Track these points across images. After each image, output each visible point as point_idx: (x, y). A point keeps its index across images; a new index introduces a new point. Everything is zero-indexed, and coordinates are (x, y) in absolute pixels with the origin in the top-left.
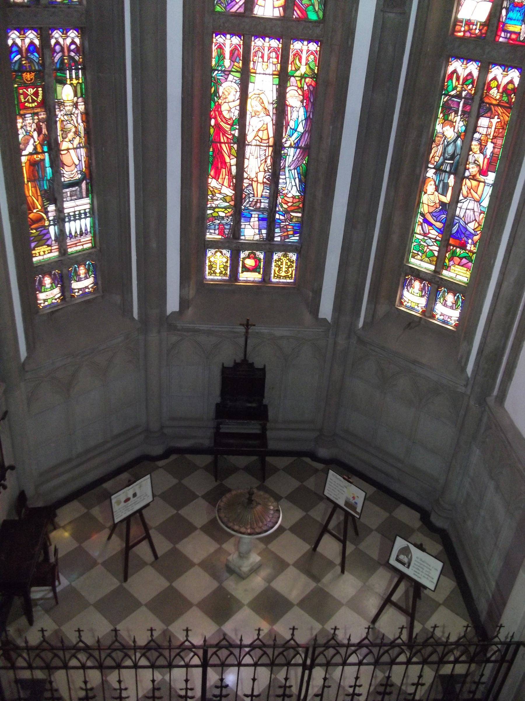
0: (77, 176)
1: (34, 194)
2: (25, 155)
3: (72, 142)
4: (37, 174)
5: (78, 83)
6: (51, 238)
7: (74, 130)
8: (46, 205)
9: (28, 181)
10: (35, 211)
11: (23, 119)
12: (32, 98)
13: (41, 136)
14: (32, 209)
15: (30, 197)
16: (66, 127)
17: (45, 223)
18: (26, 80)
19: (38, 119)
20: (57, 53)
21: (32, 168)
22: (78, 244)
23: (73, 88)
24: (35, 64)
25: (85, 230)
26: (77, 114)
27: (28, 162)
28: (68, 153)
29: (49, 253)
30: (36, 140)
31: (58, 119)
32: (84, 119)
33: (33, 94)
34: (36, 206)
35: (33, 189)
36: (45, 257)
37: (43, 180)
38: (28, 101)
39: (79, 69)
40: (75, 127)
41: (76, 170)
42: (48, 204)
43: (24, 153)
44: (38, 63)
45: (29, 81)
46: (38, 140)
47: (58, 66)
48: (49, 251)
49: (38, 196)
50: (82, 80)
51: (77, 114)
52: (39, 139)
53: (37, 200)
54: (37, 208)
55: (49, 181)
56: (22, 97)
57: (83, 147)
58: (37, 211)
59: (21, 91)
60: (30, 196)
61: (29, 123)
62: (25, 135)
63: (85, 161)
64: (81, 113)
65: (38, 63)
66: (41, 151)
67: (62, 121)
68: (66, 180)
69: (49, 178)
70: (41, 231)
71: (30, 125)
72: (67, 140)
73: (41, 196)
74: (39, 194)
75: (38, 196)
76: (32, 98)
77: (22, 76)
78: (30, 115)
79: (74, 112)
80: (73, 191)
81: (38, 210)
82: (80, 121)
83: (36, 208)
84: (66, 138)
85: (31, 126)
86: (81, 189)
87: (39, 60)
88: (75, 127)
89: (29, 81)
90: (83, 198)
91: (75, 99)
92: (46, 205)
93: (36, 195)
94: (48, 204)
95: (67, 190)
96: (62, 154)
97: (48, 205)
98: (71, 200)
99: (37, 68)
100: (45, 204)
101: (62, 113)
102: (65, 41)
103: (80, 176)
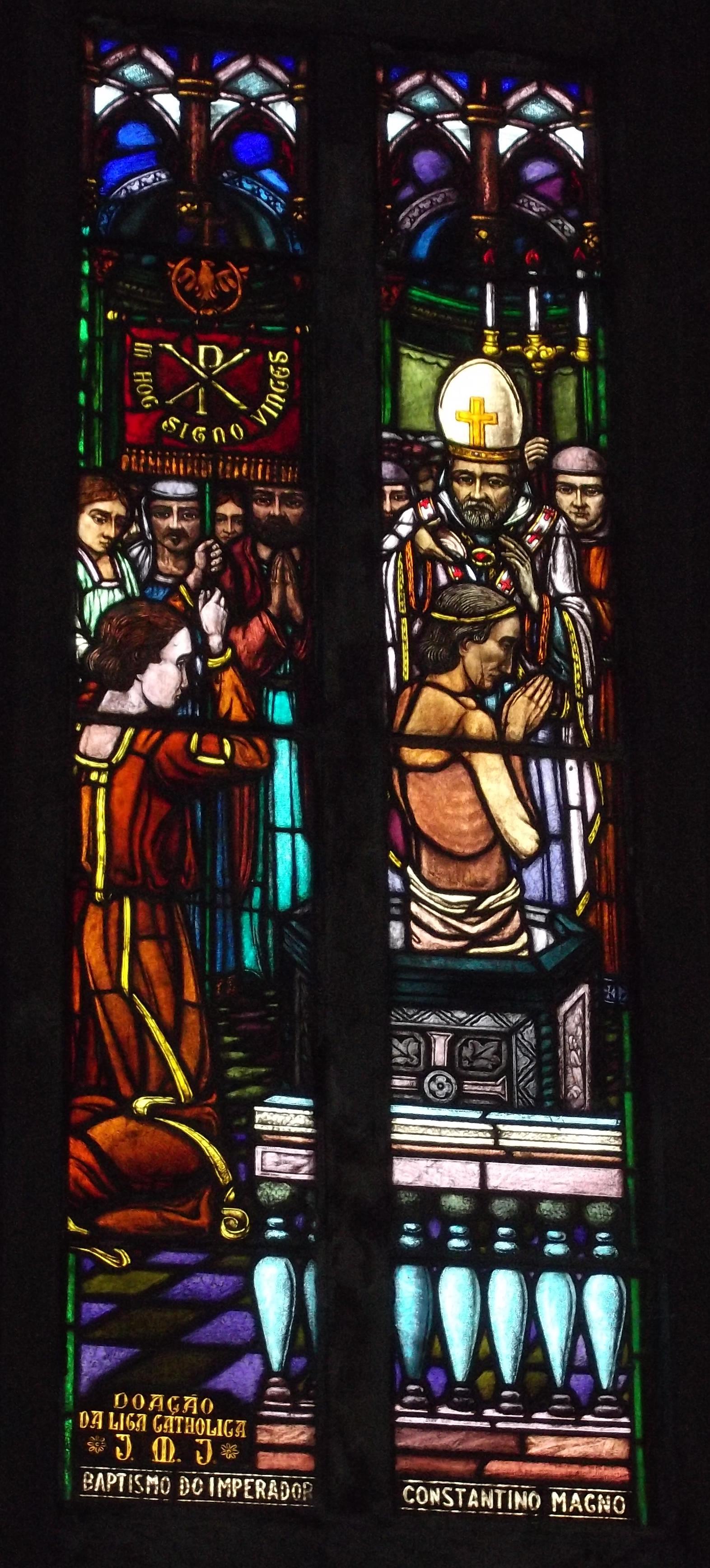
0: (524, 938)
1: (149, 983)
2: (121, 720)
3: (491, 702)
4: (190, 857)
5: (565, 359)
6: (258, 1344)
7: (508, 628)
8: (238, 1084)
9: (114, 891)
10: (142, 1104)
11: (131, 504)
12: (215, 401)
13: (256, 630)
14: (126, 1090)
15: (113, 1000)
16: (448, 599)
17: (217, 1218)
18: (191, 297)
19: (247, 519)
20: (422, 189)
21: (160, 809)
22: (495, 1467)
23: (525, 384)
24: (264, 224)
25: (570, 1368)
26: (548, 538)
27: (135, 766)
28: (460, 771)
29: (221, 1465)
30: (215, 641)
31: (390, 542)
32: (597, 576)
33: (228, 377)
34: (154, 1069)
35: (149, 951)
36: (188, 1486)
37: (239, 905)
38: (186, 411)
39: (579, 286)
40: (524, 610)
41: (511, 893)
42: (255, 1080)
43: (110, 702)
44: (278, 224)
45: (208, 304)
46: (227, 642)
47: (422, 247)
48: (230, 1453)
49: (180, 1005)
50: (592, 348)
51: (548, 538)
52: (237, 636)
53: (174, 1037)
54: (167, 1086)
55: (282, 919)
56: (143, 377)
57: (582, 755)
58: (154, 1109)
59: (143, 349)
60: (116, 987)
61: (178, 534)
62: (129, 599)
63: (589, 850)
64: (575, 535)
65: (278, 224)
66: (237, 713)
67: (423, 559)
68: (425, 941)
69: (284, 899)
70: (181, 1272)
71: (181, 546)
72: (454, 680)
73: (205, 1005)
74: (190, 993)
75: (180, 1005)
76: (215, 401)
77: (160, 269)
78: (184, 489)
79: (525, 523)
80: (484, 1036)
81: (168, 1100)
82: (562, 582)
83: (153, 1085)
84: (447, 667)
85: (188, 556)
86: (554, 1036)
87: (291, 207)
88: (524, 610)
89: (208, 304)
90: (562, 1107)
91: (535, 448)
92: (238, 1084)
93: (163, 994)
94: (255, 1080)
95: (432, 1019)
96: (406, 769)
97: (253, 1090)
98: (459, 1100)
99: (269, 241)
100: (234, 1073)
101: (426, 512)
102: (485, 141)
103: (541, 939)
